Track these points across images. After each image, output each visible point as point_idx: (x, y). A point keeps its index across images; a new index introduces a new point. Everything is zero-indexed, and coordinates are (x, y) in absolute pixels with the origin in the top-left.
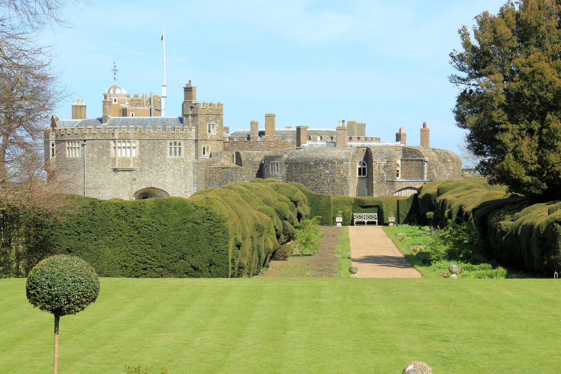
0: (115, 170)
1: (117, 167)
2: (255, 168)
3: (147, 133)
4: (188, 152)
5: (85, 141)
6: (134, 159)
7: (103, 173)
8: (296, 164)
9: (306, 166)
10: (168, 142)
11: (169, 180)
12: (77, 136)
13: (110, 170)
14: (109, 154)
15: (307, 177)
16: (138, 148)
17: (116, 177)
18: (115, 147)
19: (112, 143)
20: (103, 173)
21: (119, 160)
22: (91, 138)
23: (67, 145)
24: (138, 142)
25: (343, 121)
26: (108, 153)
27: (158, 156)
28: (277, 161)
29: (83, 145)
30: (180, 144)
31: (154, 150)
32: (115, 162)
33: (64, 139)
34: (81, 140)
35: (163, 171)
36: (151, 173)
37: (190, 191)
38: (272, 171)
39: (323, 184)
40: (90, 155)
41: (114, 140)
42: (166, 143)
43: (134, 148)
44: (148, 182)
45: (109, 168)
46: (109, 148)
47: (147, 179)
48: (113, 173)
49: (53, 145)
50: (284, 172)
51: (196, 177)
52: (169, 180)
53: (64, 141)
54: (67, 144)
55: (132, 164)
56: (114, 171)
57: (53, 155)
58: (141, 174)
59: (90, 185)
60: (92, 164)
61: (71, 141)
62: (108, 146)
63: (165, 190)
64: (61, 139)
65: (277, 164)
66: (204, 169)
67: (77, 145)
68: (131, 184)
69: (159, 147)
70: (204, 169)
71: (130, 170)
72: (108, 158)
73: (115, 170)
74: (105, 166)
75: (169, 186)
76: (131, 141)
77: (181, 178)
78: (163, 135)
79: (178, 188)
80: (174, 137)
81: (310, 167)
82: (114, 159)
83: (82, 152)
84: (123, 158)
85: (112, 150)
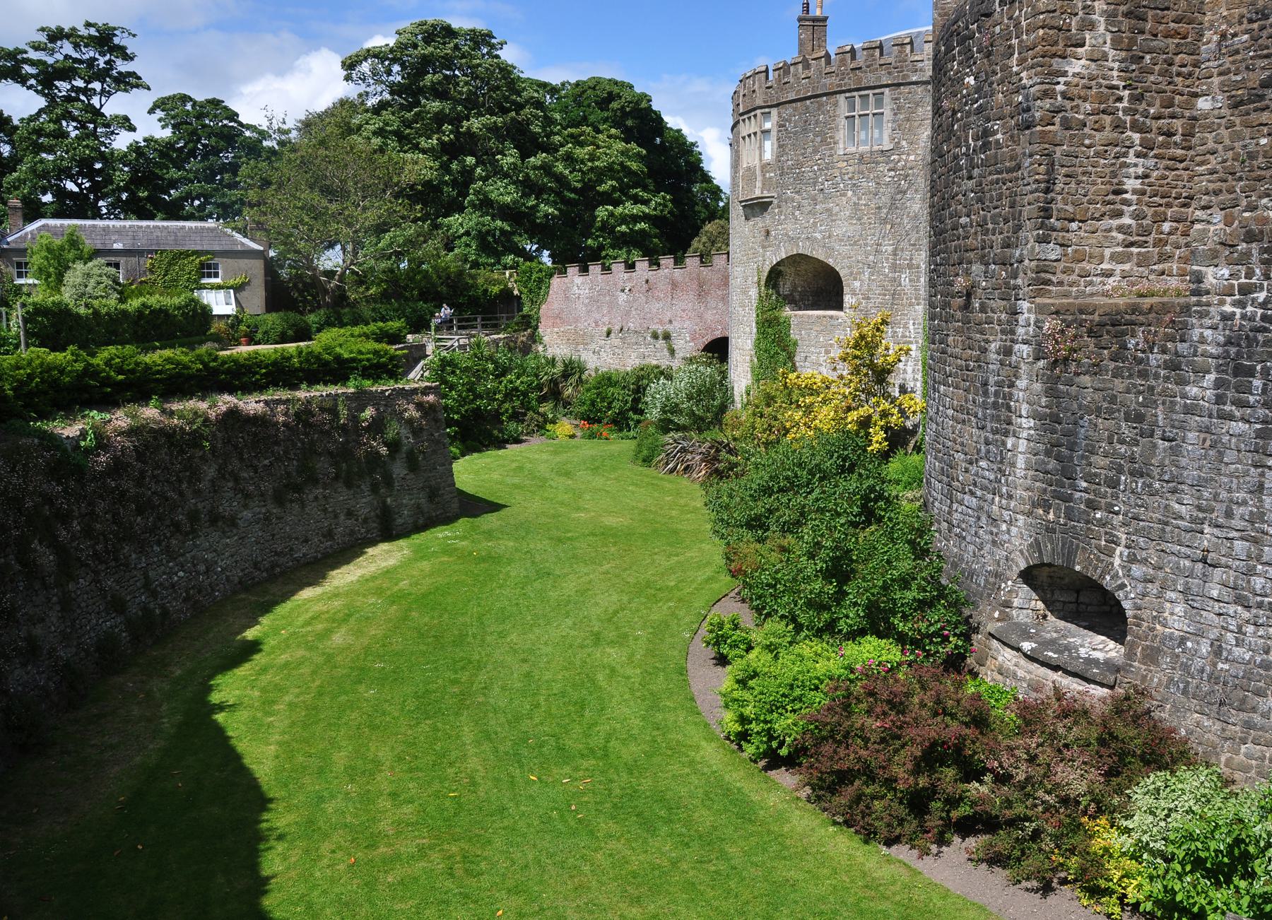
3: (792, 80)
4: (904, 126)
6: (765, 167)
10: (841, 98)
11: (843, 228)
16: (774, 133)
24: (774, 112)
27: (816, 151)
30: (879, 103)
31: (805, 130)
35: (827, 198)
37: (910, 266)
42: (836, 104)
43: (767, 132)
47: (789, 227)
52: (843, 228)
55: (759, 184)
69: (817, 122)
75: (845, 249)
76: (758, 112)
77: (884, 221)
78: (828, 81)
79: (867, 254)
80: (860, 80)
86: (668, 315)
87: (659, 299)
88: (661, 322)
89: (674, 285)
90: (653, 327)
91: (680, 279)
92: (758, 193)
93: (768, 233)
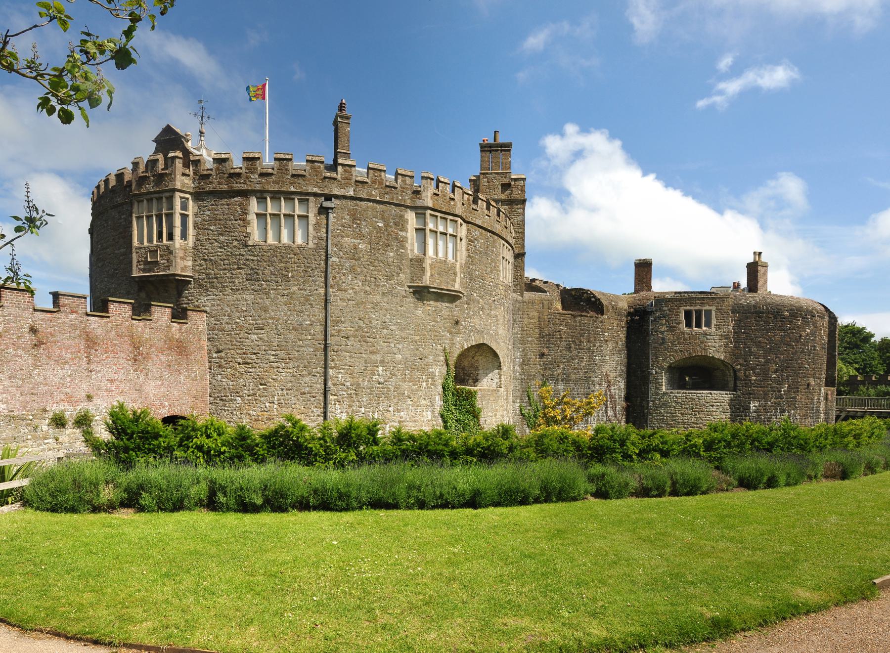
0: (421, 293)
1: (427, 280)
2: (621, 321)
5: (329, 198)
7: (384, 295)
8: (756, 312)
9: (775, 317)
12: (301, 181)
13: (402, 290)
14: (403, 246)
15: (778, 338)
17: (419, 312)
18: (421, 231)
19: (411, 217)
20: (384, 295)
21: (431, 265)
22: (351, 193)
23: (254, 206)
25: (760, 253)
26: (402, 242)
28: (707, 308)
29: (324, 211)
32: (423, 270)
33: (244, 187)
34: (316, 195)
36: (482, 309)
38: (689, 324)
39: (802, 352)
40: (347, 241)
41: (421, 211)
44: (478, 331)
45: (401, 284)
46: (404, 229)
48: (411, 299)
49: (184, 207)
50: (730, 326)
51: (517, 329)
53: (245, 194)
54: (254, 202)
56: (414, 293)
57: (184, 236)
58: (469, 309)
59: (347, 328)
60: (352, 269)
61: (276, 196)
62: (401, 224)
63: (498, 351)
64: (225, 187)
65: (708, 313)
66: (536, 314)
67: (299, 210)
68: (451, 333)
70: (536, 314)
71: (453, 297)
72: (401, 257)
73: (421, 293)
74: (389, 278)
81: (783, 319)
82: (418, 263)
83: (317, 230)
84: (441, 262)
85: (411, 234)
86: (85, 387)
87: (61, 362)
88: (70, 399)
89: (91, 342)
90: (54, 408)
91: (100, 333)
92: (457, 287)
93: (457, 322)
